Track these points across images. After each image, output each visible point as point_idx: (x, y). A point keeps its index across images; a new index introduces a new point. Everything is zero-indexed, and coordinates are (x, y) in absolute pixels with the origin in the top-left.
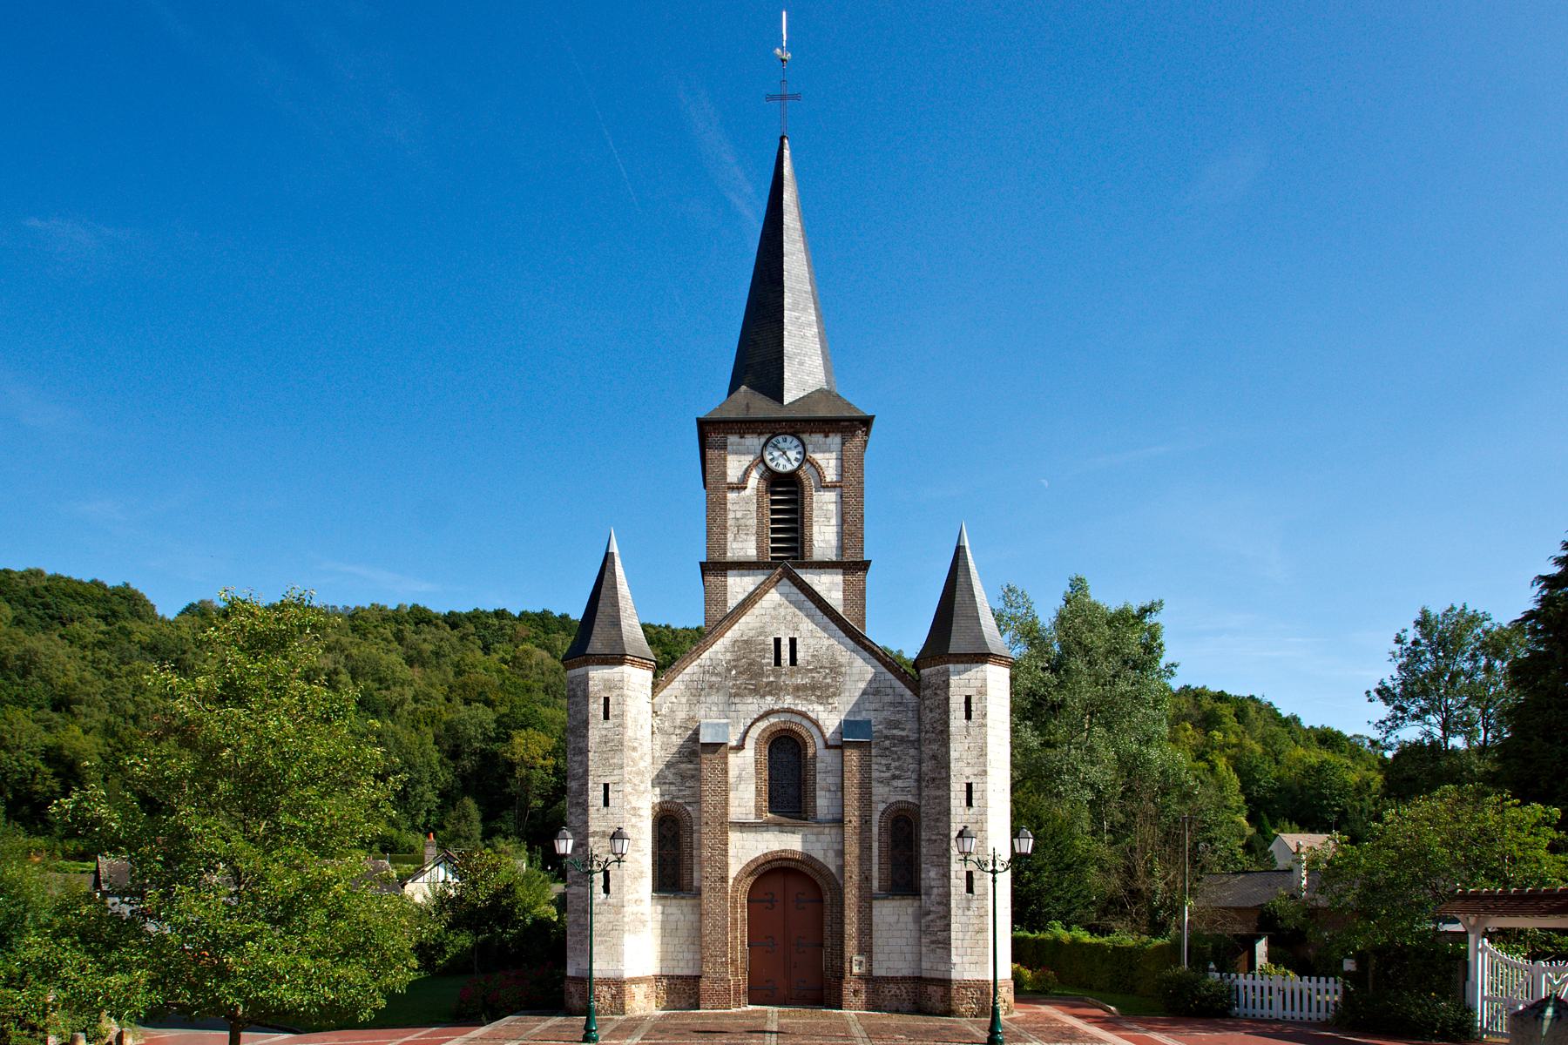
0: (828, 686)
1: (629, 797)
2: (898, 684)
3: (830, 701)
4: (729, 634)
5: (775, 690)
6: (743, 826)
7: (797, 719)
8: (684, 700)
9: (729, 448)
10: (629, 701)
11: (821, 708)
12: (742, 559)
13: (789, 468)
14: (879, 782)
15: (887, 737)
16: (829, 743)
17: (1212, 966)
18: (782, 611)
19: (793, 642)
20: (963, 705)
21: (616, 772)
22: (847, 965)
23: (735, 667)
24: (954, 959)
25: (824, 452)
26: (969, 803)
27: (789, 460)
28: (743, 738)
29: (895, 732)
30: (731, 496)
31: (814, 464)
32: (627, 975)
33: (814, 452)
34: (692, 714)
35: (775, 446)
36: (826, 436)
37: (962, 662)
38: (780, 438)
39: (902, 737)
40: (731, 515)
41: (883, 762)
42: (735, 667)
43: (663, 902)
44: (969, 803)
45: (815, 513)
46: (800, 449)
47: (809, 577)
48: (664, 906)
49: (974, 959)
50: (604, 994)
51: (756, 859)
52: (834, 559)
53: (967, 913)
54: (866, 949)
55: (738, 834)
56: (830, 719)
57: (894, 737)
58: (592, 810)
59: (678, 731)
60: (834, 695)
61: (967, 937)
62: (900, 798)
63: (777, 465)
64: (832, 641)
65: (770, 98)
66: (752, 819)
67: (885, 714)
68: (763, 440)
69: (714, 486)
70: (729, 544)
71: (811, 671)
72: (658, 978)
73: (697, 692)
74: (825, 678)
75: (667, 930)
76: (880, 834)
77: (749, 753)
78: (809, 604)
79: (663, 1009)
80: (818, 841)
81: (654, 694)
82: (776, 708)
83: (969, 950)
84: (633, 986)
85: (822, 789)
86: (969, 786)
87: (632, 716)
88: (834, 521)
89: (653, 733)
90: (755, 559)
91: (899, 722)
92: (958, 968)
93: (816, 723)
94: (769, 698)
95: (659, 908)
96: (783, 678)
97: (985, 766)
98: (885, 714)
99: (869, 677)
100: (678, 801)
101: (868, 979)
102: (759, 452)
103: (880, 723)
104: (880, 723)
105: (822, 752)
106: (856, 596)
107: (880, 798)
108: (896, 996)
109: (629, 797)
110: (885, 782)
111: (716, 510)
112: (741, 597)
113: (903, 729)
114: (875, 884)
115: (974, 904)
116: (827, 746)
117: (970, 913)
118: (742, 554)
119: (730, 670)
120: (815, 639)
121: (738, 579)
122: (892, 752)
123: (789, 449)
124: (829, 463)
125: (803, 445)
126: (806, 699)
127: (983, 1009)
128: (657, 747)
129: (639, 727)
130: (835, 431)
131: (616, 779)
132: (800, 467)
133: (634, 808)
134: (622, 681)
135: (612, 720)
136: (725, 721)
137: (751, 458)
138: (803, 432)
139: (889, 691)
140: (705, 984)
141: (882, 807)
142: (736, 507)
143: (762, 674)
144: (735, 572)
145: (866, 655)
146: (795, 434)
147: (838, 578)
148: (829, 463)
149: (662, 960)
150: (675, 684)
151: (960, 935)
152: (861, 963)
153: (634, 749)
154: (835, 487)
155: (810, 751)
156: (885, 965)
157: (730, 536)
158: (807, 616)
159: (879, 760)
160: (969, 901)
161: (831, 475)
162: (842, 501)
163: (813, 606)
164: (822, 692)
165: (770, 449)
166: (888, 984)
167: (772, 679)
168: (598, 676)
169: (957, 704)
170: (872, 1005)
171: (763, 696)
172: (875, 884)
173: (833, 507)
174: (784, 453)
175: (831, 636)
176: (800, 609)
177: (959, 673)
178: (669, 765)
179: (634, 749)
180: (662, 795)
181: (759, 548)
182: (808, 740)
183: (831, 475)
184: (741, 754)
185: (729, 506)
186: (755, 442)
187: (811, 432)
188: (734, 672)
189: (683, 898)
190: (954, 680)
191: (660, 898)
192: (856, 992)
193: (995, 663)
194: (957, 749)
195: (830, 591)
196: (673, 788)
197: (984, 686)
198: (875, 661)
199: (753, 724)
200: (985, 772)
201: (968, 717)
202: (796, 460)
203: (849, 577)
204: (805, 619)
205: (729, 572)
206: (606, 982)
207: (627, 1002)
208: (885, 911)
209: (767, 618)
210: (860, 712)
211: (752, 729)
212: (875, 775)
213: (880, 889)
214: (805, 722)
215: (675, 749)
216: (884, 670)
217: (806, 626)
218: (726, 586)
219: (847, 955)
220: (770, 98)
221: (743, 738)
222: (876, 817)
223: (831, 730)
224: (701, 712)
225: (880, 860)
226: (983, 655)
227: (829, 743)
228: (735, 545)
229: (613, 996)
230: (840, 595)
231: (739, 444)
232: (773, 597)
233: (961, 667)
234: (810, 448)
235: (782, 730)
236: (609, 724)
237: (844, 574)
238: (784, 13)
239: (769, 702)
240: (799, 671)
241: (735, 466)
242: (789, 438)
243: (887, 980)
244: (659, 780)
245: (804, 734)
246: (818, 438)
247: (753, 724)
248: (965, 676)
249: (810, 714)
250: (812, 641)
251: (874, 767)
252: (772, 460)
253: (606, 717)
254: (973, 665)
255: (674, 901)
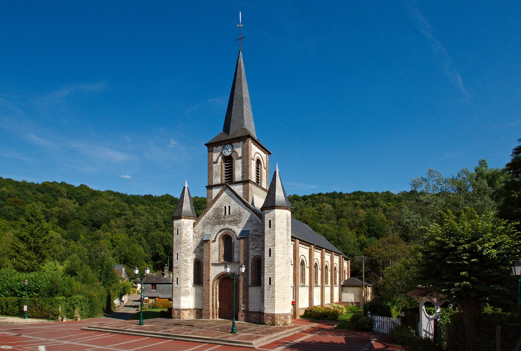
0: (238, 220)
1: (183, 257)
2: (257, 217)
3: (238, 225)
4: (213, 207)
5: (223, 223)
6: (215, 265)
7: (229, 231)
8: (201, 228)
9: (214, 151)
10: (183, 230)
11: (236, 227)
12: (217, 184)
13: (229, 154)
14: (251, 249)
15: (254, 235)
16: (238, 238)
17: (369, 312)
18: (226, 198)
19: (229, 207)
20: (269, 223)
21: (180, 250)
22: (240, 307)
23: (214, 216)
24: (265, 306)
25: (238, 148)
26: (270, 256)
27: (229, 152)
28: (215, 238)
29: (256, 233)
30: (214, 165)
31: (236, 152)
32: (182, 308)
33: (236, 148)
34: (203, 231)
35: (225, 148)
36: (239, 143)
37: (268, 209)
38: (226, 146)
39: (258, 234)
40: (214, 171)
41: (253, 243)
42: (214, 216)
43: (196, 287)
44: (270, 256)
45: (236, 167)
46: (232, 148)
47: (233, 187)
48: (196, 288)
49: (271, 306)
50: (176, 312)
51: (219, 274)
52: (241, 180)
53: (269, 291)
54: (246, 303)
55: (214, 267)
56: (238, 230)
57: (256, 235)
58: (174, 261)
59: (200, 237)
60: (240, 223)
61: (269, 299)
62: (257, 254)
63: (226, 154)
64: (240, 206)
65: (237, 40)
66: (217, 262)
67: (253, 227)
68: (222, 147)
69: (211, 163)
70: (214, 180)
71: (233, 216)
72: (194, 309)
73: (204, 225)
74: (237, 218)
75: (197, 295)
76: (251, 266)
77: (217, 242)
78: (234, 195)
79: (195, 318)
80: (234, 268)
81: (194, 227)
82: (224, 228)
83: (269, 303)
84: (184, 311)
85: (236, 252)
86: (270, 250)
87: (185, 233)
88: (241, 169)
89: (194, 238)
90: (220, 183)
91: (257, 230)
92: (266, 309)
93: (234, 232)
94: (222, 225)
95: (195, 289)
96: (226, 219)
97: (275, 243)
98: (253, 227)
99: (249, 216)
100: (200, 257)
101: (247, 312)
102: (221, 151)
103: (252, 231)
104: (252, 231)
105: (236, 241)
106: (246, 191)
107: (252, 254)
108: (255, 318)
109: (183, 257)
110: (253, 249)
111: (210, 169)
112: (216, 195)
113: (258, 232)
114: (250, 282)
115: (271, 288)
116: (237, 239)
117: (270, 291)
118: (217, 182)
119: (213, 218)
120: (235, 206)
121: (215, 190)
122: (255, 239)
123: (229, 148)
124: (239, 151)
125: (233, 146)
126: (232, 225)
127: (273, 323)
128: (195, 242)
129: (187, 237)
130: (241, 141)
131: (179, 252)
132: (232, 154)
133: (185, 260)
134: (181, 224)
135: (179, 235)
136: (211, 233)
137: (219, 153)
138: (233, 143)
139: (255, 220)
140: (203, 311)
141: (252, 257)
142: (216, 168)
143: (220, 218)
144: (215, 188)
145: (249, 209)
146: (231, 144)
147: (241, 186)
148: (239, 151)
149: (195, 304)
150: (199, 223)
151: (267, 299)
152: (243, 307)
153: (185, 243)
154: (241, 158)
155: (233, 241)
156: (253, 307)
157: (214, 177)
158: (233, 199)
159: (252, 242)
160: (270, 287)
161: (240, 155)
162: (243, 163)
163: (235, 195)
164: (236, 222)
165: (224, 149)
166: (253, 314)
167: (223, 219)
168: (176, 222)
169: (267, 223)
170: (247, 320)
171: (220, 225)
172: (250, 282)
173: (240, 164)
174: (227, 150)
175: (239, 204)
176: (231, 197)
177: (267, 213)
178: (198, 247)
179: (185, 243)
180: (196, 256)
181: (221, 180)
182: (232, 237)
183: (240, 155)
184: (215, 243)
185: (214, 168)
186: (220, 148)
187: (235, 142)
188: (213, 218)
189: (200, 286)
190: (266, 216)
191: (195, 286)
192: (242, 316)
193: (279, 209)
194: (267, 238)
195: (239, 190)
196: (198, 254)
197: (274, 216)
198: (251, 211)
199: (218, 233)
200: (275, 245)
201: (270, 227)
202: (231, 151)
203: (244, 186)
204: (233, 200)
205: (213, 188)
206: (177, 309)
207: (181, 316)
208: (253, 290)
209: (222, 201)
210: (246, 227)
211: (218, 235)
212: (250, 247)
213: (251, 283)
214: (231, 232)
215: (199, 242)
216: (253, 213)
217: (233, 202)
218: (212, 192)
219: (240, 304)
220: (237, 40)
221: (215, 238)
222: (250, 260)
223: (238, 234)
224: (205, 231)
225: (251, 274)
226: (273, 206)
227: (238, 238)
228: (215, 180)
229: (178, 314)
230: (242, 191)
231: (216, 149)
232: (224, 194)
233: (268, 211)
234: (234, 147)
235: (225, 235)
236: (178, 236)
237: (243, 185)
238: (240, 13)
239: (222, 227)
240: (230, 216)
241: (215, 156)
242: (229, 145)
243: (253, 312)
244: (195, 252)
245: (231, 235)
246: (237, 144)
247: (218, 233)
248: (269, 214)
249: (233, 229)
250: (234, 207)
251: (250, 244)
252: (224, 153)
253: (178, 234)
254: (271, 210)
255: (198, 287)
